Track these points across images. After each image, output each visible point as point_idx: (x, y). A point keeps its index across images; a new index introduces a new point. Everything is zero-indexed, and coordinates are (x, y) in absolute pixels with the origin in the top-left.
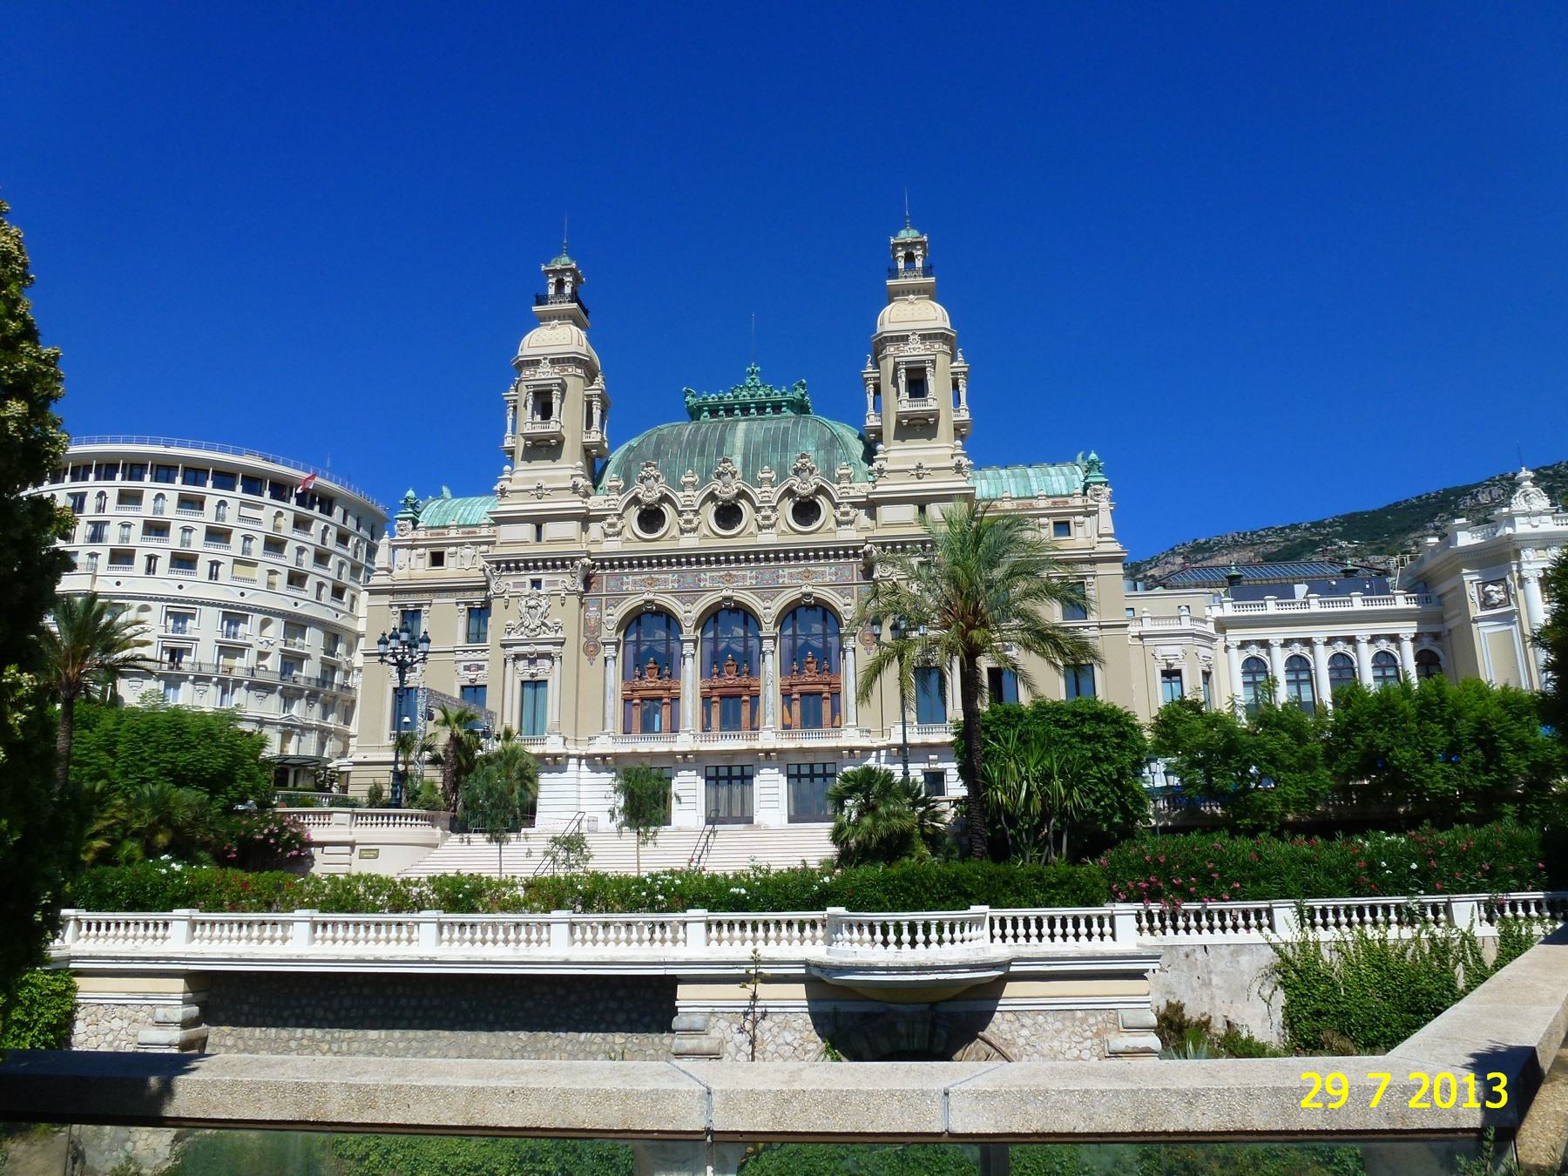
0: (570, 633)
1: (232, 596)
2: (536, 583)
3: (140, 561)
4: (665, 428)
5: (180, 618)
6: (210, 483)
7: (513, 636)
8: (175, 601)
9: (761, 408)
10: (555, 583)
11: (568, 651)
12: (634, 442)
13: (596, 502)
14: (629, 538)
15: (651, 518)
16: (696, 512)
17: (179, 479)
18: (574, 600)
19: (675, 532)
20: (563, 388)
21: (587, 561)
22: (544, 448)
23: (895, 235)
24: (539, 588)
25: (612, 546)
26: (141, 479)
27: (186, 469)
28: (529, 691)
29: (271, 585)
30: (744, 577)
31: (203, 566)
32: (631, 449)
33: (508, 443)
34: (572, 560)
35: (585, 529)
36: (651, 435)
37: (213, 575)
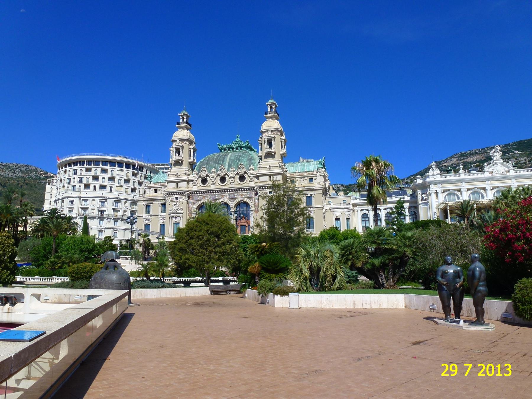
0: (184, 211)
1: (116, 196)
2: (177, 198)
3: (92, 187)
4: (211, 155)
5: (103, 202)
7: (171, 212)
11: (184, 215)
12: (202, 160)
13: (191, 177)
14: (199, 186)
15: (204, 181)
16: (215, 179)
18: (186, 202)
19: (210, 184)
20: (183, 147)
21: (188, 193)
22: (178, 163)
25: (195, 189)
28: (175, 225)
29: (126, 192)
31: (108, 188)
32: (201, 162)
33: (171, 162)
35: (188, 184)
36: (207, 157)
37: (111, 190)
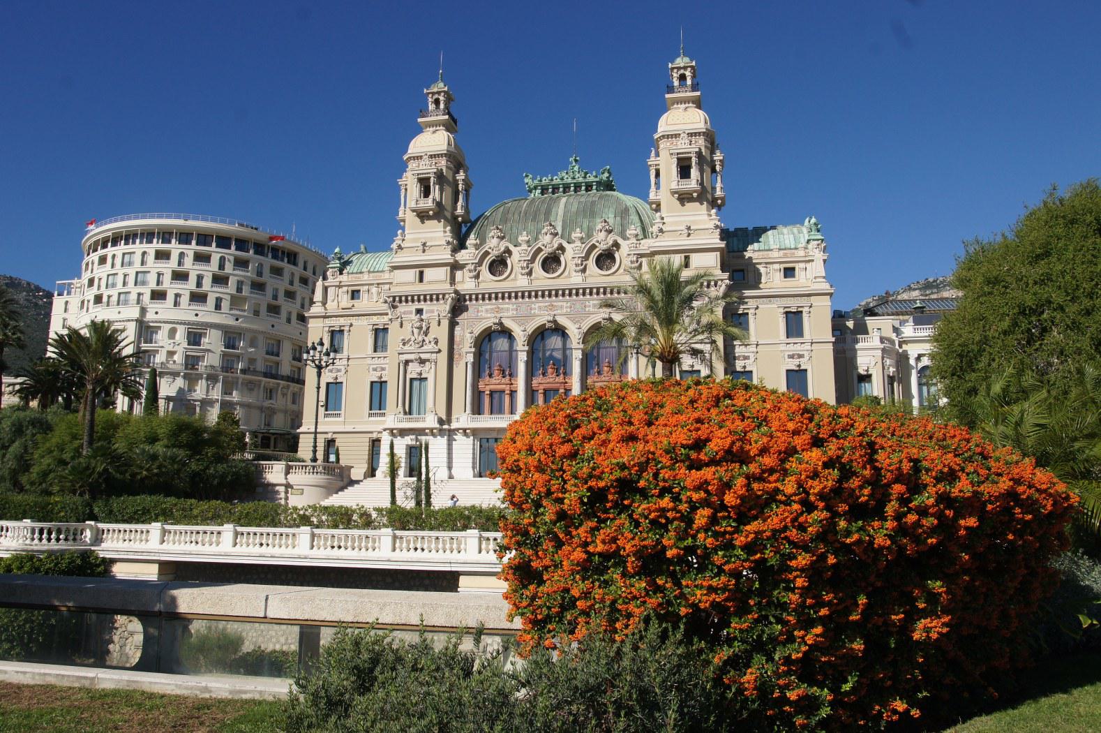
2: (419, 311)
6: (214, 244)
8: (193, 324)
9: (577, 187)
10: (432, 311)
17: (194, 242)
23: (672, 62)
24: (422, 314)
26: (169, 242)
27: (199, 235)
30: (562, 307)
34: (444, 295)
